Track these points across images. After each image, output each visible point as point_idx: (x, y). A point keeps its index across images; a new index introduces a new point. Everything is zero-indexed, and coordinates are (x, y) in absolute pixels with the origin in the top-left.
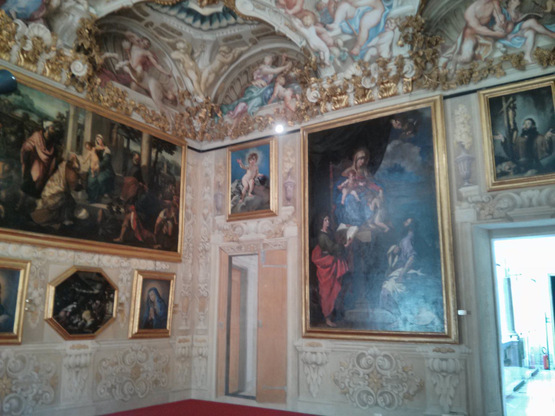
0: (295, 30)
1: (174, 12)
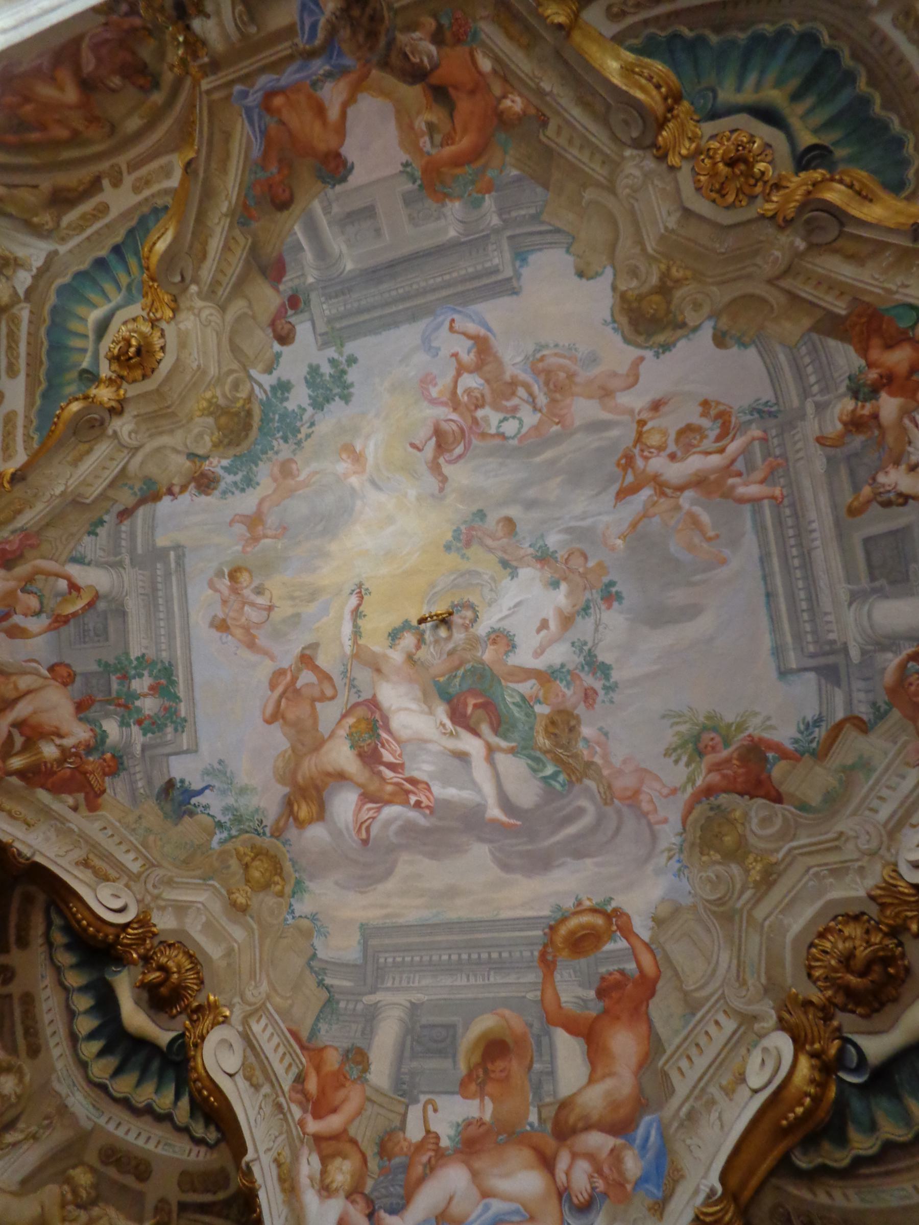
0: (289, 1186)
1: (74, 979)
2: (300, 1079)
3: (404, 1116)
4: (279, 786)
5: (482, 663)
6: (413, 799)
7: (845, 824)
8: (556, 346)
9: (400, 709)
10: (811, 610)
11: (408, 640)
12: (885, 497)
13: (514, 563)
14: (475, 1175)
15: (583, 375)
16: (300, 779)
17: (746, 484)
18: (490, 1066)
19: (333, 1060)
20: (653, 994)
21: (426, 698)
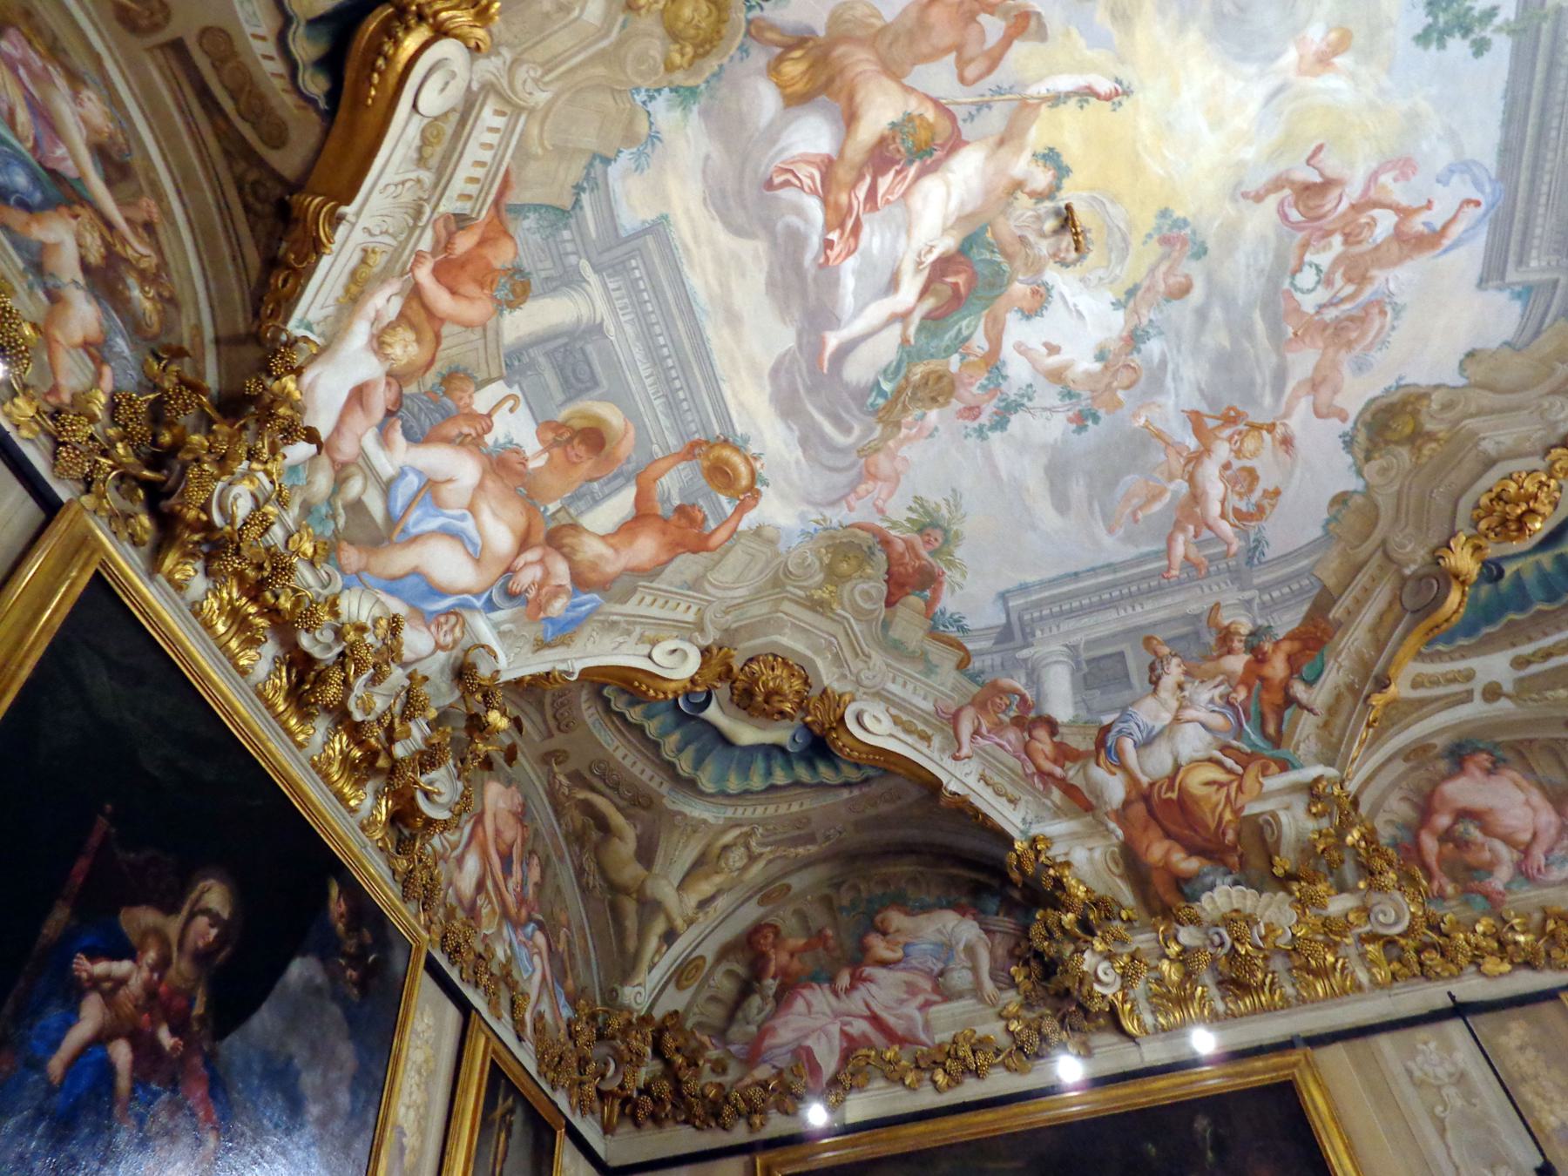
2: (461, 221)
3: (490, 381)
4: (825, 16)
5: (1010, 281)
6: (834, 236)
7: (877, 659)
8: (1393, 328)
9: (948, 185)
10: (1062, 613)
11: (1041, 178)
12: (1158, 666)
13: (1131, 304)
14: (480, 486)
15: (1345, 359)
16: (840, 50)
17: (1186, 543)
18: (576, 441)
19: (502, 256)
20: (694, 552)
21: (963, 219)
